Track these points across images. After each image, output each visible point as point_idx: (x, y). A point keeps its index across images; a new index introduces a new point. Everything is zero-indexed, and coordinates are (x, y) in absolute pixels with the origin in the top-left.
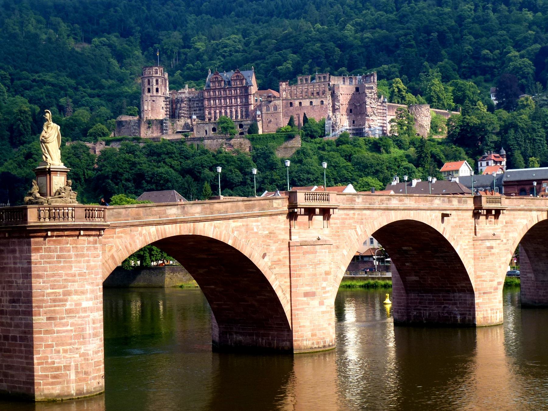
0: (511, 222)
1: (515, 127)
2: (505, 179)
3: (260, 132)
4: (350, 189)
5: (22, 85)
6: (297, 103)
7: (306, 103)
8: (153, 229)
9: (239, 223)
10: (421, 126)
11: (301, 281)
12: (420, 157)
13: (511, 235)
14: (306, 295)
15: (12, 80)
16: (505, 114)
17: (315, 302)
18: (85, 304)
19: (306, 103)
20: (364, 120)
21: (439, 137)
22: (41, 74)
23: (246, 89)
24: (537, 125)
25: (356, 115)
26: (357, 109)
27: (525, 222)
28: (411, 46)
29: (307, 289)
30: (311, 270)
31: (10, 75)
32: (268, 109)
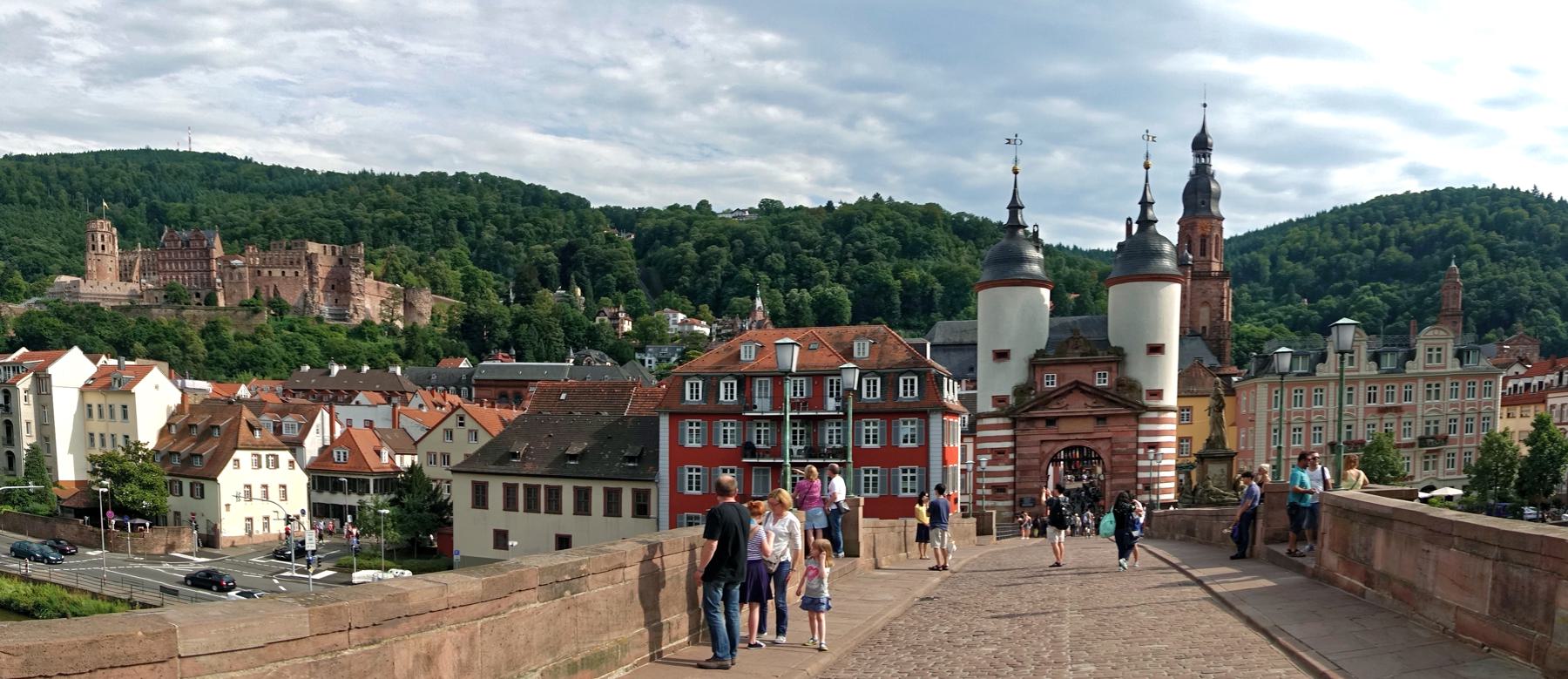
1: (529, 321)
2: (476, 376)
3: (221, 303)
6: (266, 272)
7: (277, 273)
10: (421, 314)
12: (409, 349)
16: (518, 308)
19: (277, 273)
20: (349, 299)
21: (438, 330)
23: (207, 251)
24: (555, 323)
25: (340, 292)
26: (340, 286)
28: (427, 231)
32: (231, 277)
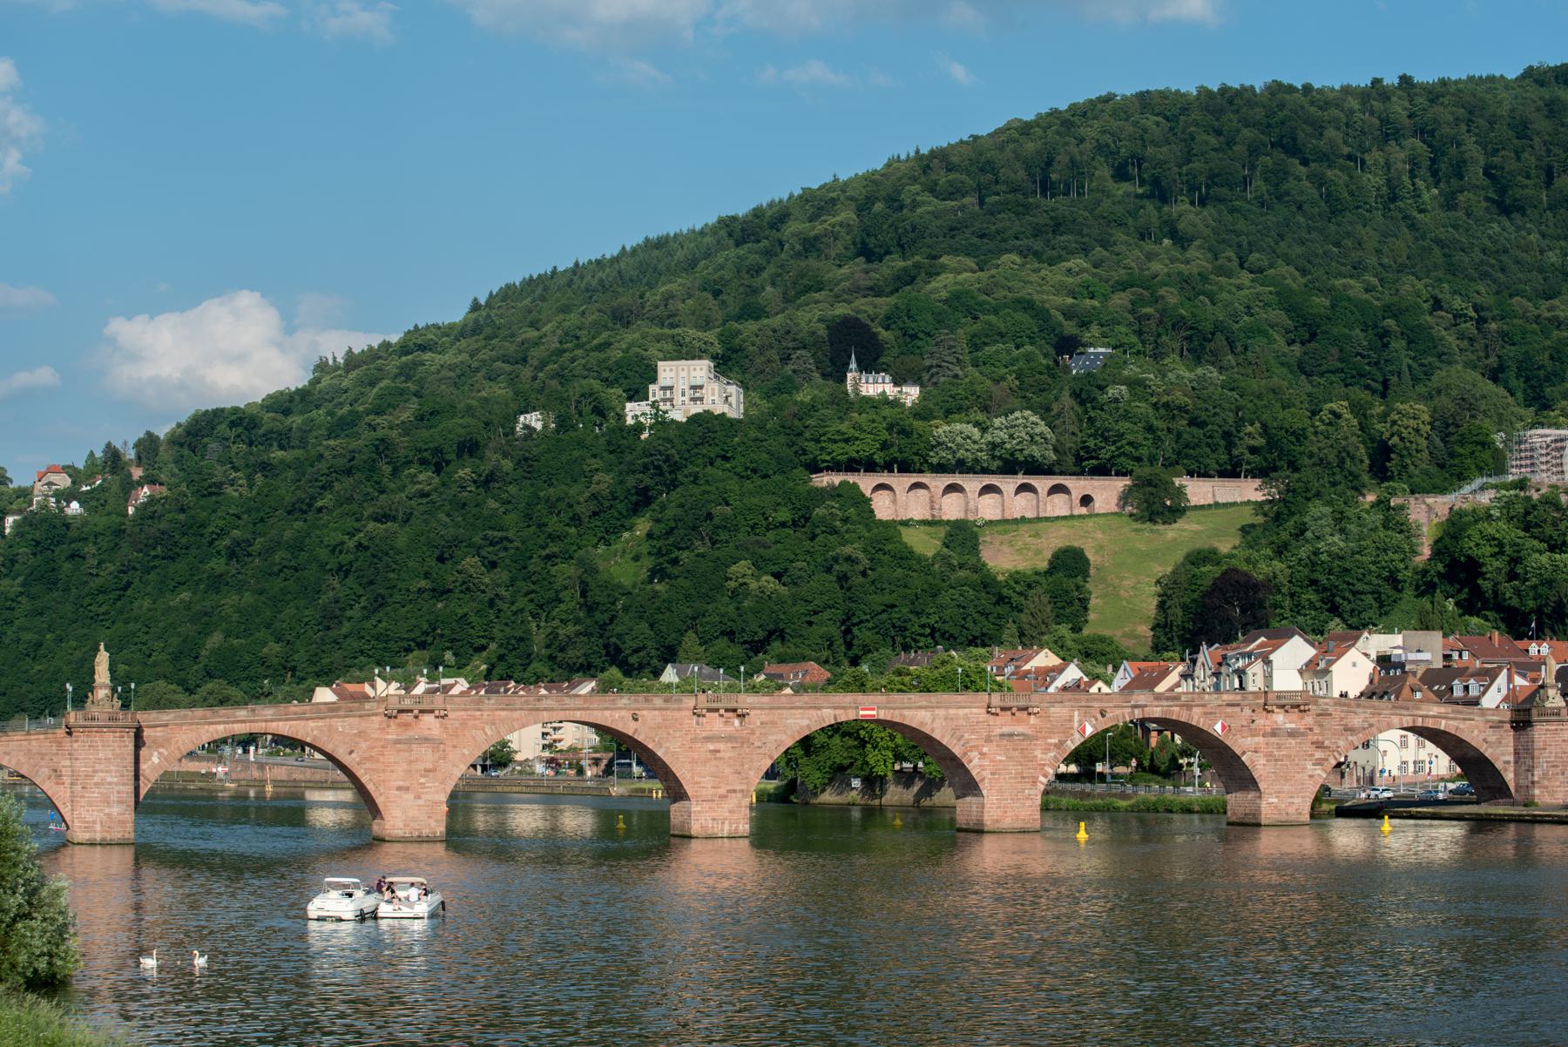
0: (773, 723)
4: (587, 687)
5: (1503, 335)
8: (221, 727)
9: (320, 723)
11: (394, 776)
13: (771, 738)
14: (399, 788)
15: (1481, 321)
17: (410, 796)
18: (109, 779)
22: (1556, 302)
27: (806, 722)
29: (401, 783)
30: (405, 766)
31: (1476, 308)
